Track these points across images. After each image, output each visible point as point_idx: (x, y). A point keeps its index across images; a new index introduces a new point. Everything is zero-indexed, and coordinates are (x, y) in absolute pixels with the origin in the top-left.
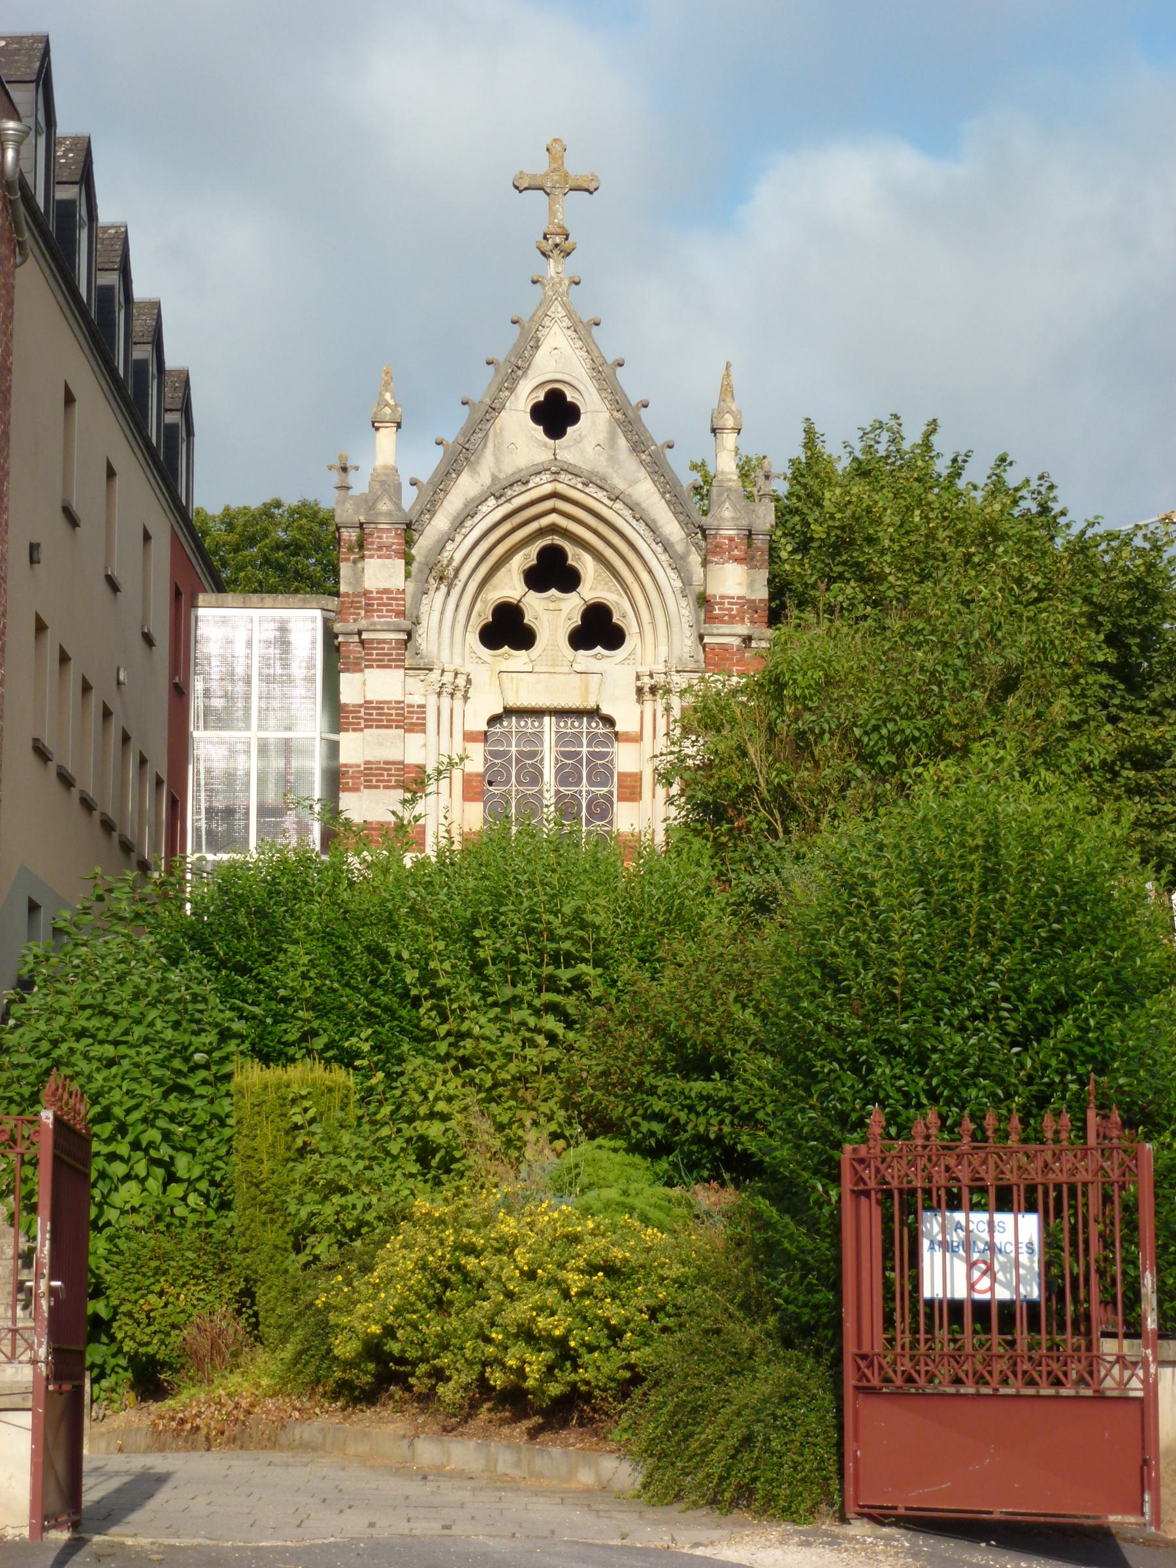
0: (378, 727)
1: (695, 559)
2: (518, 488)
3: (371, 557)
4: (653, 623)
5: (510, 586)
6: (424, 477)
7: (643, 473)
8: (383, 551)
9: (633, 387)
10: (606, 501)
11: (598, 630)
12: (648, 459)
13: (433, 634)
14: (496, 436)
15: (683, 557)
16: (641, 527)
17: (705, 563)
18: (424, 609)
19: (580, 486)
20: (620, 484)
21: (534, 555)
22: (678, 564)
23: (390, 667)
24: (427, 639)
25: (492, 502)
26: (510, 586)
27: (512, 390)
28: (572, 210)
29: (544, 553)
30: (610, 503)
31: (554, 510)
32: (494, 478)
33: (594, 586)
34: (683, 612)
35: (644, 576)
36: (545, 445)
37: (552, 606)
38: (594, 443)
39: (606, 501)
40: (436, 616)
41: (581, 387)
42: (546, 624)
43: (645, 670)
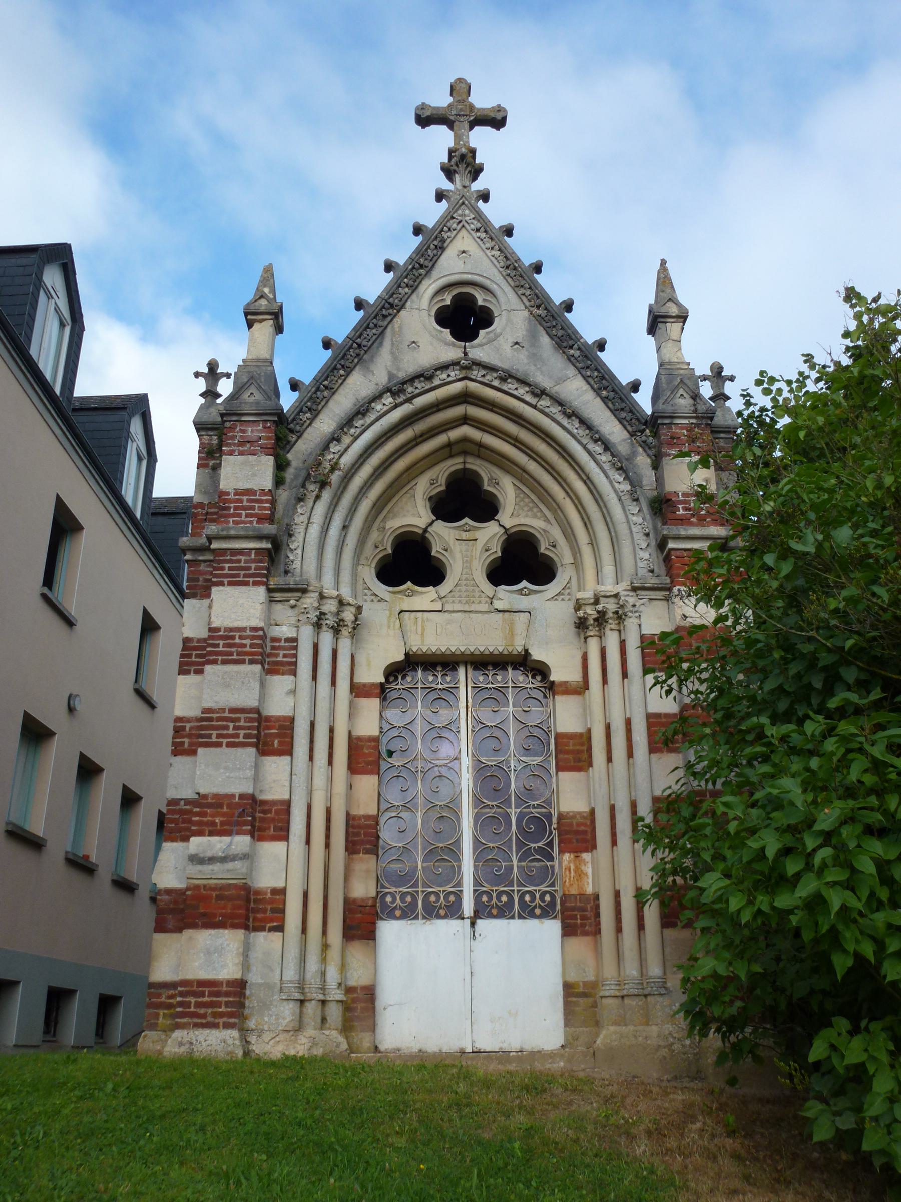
0: (224, 662)
1: (643, 461)
2: (420, 385)
3: (231, 453)
4: (593, 543)
5: (415, 514)
6: (307, 377)
7: (571, 371)
8: (247, 446)
9: (556, 288)
10: (528, 398)
11: (521, 563)
12: (577, 353)
13: (311, 552)
14: (394, 333)
15: (630, 458)
16: (573, 425)
17: (656, 466)
18: (298, 519)
19: (496, 383)
20: (545, 382)
21: (443, 480)
22: (623, 467)
23: (246, 584)
24: (305, 555)
25: (388, 400)
26: (415, 514)
27: (414, 289)
28: (481, 139)
29: (457, 299)
30: (533, 401)
31: (465, 420)
32: (391, 376)
33: (515, 511)
34: (633, 522)
35: (579, 486)
36: (454, 345)
37: (464, 536)
38: (511, 340)
39: (528, 398)
40: (315, 530)
41: (493, 287)
42: (458, 556)
43: (587, 595)
